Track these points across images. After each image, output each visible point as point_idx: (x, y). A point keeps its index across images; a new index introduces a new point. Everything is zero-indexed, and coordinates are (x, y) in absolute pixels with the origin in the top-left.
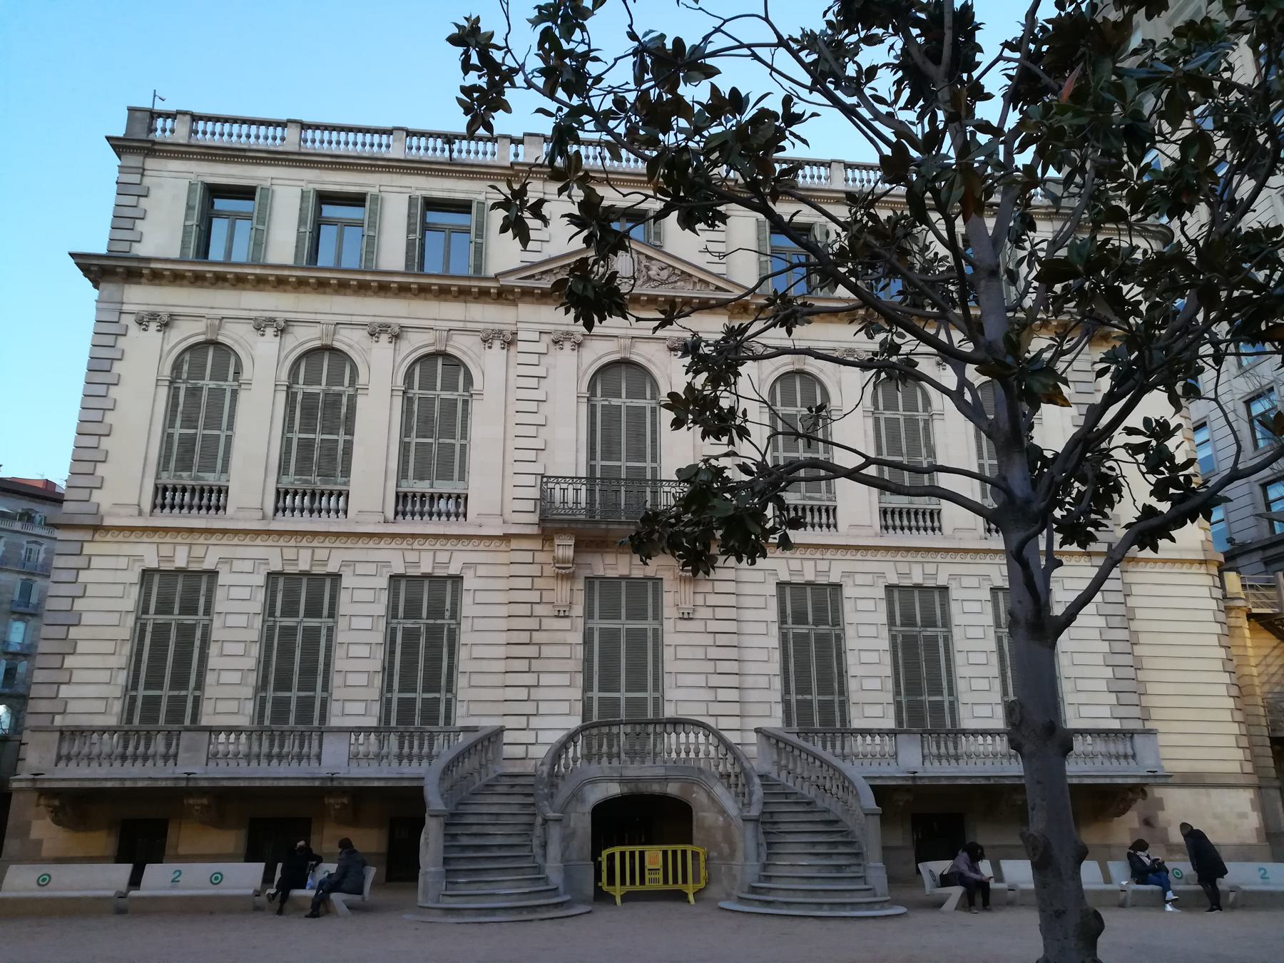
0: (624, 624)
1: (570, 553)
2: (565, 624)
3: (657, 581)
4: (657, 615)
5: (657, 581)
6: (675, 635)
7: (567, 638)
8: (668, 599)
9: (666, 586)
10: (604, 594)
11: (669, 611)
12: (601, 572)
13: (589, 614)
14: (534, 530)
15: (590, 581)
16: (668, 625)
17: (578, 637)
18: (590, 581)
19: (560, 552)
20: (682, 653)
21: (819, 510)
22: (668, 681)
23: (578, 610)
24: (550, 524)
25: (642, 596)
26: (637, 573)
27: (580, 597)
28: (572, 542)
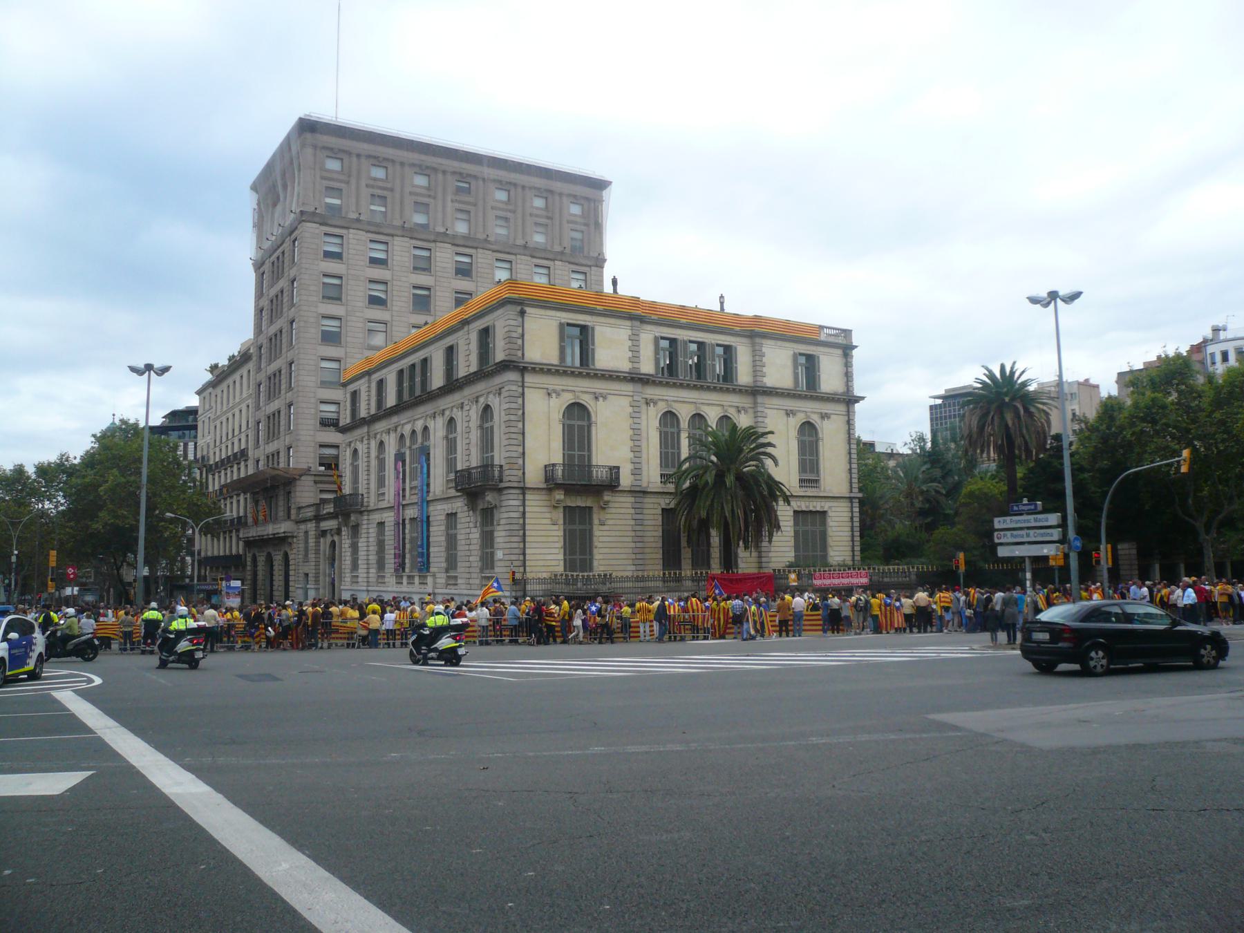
0: (577, 527)
4: (591, 524)
5: (590, 508)
6: (598, 532)
7: (557, 533)
9: (595, 510)
10: (570, 512)
11: (596, 521)
14: (543, 486)
16: (595, 528)
17: (561, 533)
19: (558, 497)
20: (601, 539)
22: (595, 551)
23: (561, 522)
24: (551, 483)
27: (561, 515)
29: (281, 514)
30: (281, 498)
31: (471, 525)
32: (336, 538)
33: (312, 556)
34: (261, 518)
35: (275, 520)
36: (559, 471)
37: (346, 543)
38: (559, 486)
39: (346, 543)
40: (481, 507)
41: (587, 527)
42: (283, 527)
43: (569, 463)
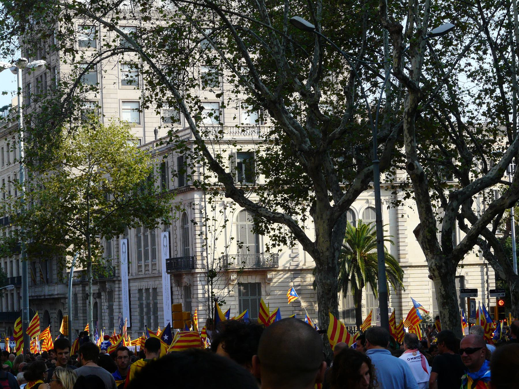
2: (233, 298)
4: (260, 294)
5: (259, 284)
9: (263, 286)
11: (263, 293)
16: (263, 297)
17: (237, 303)
26: (253, 282)
29: (55, 276)
30: (54, 262)
31: (179, 297)
32: (98, 300)
33: (80, 315)
34: (38, 279)
35: (48, 282)
37: (105, 305)
39: (105, 305)
40: (184, 285)
41: (256, 297)
42: (57, 290)
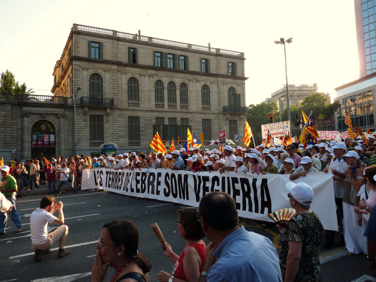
1: (87, 110)
3: (102, 116)
4: (103, 121)
5: (102, 116)
6: (106, 126)
8: (104, 119)
9: (105, 117)
10: (93, 117)
11: (105, 121)
12: (92, 114)
13: (90, 121)
15: (90, 115)
18: (90, 115)
21: (133, 103)
23: (88, 120)
25: (100, 118)
27: (89, 118)
28: (88, 109)
36: (87, 100)
38: (86, 106)
43: (92, 97)
